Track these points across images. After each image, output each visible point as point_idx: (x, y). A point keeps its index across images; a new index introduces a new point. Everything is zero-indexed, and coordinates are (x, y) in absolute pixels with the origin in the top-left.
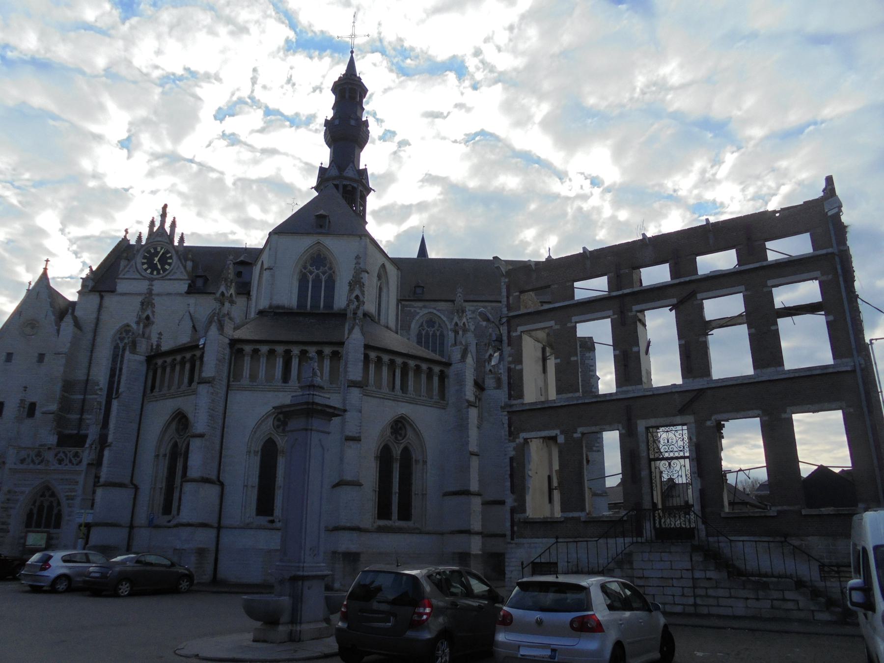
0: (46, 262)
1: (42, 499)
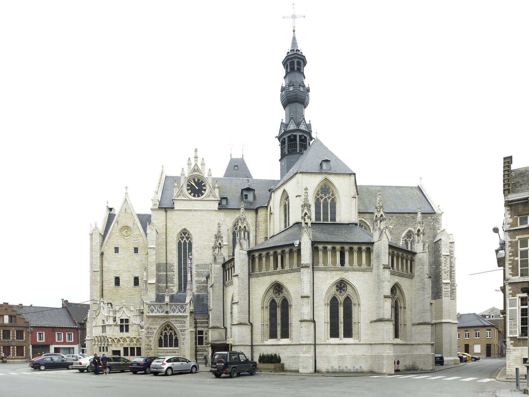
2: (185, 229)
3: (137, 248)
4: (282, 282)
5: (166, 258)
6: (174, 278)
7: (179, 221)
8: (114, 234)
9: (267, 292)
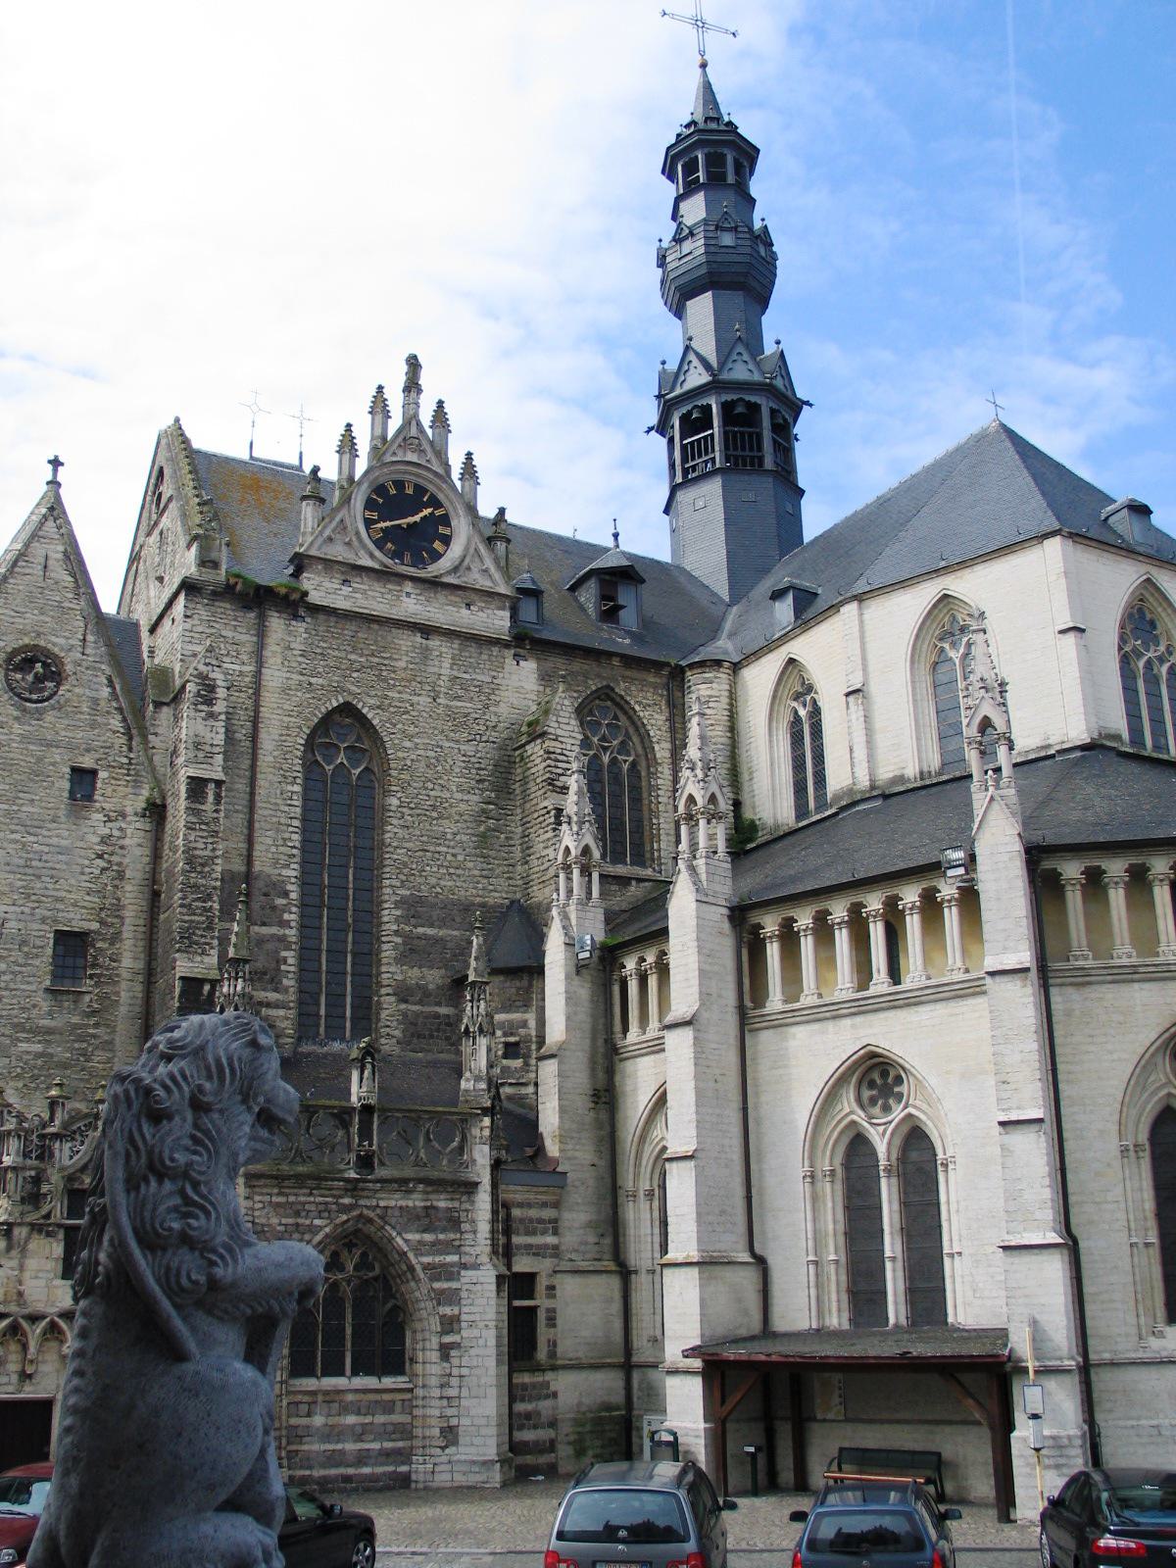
9: (1144, 1067)
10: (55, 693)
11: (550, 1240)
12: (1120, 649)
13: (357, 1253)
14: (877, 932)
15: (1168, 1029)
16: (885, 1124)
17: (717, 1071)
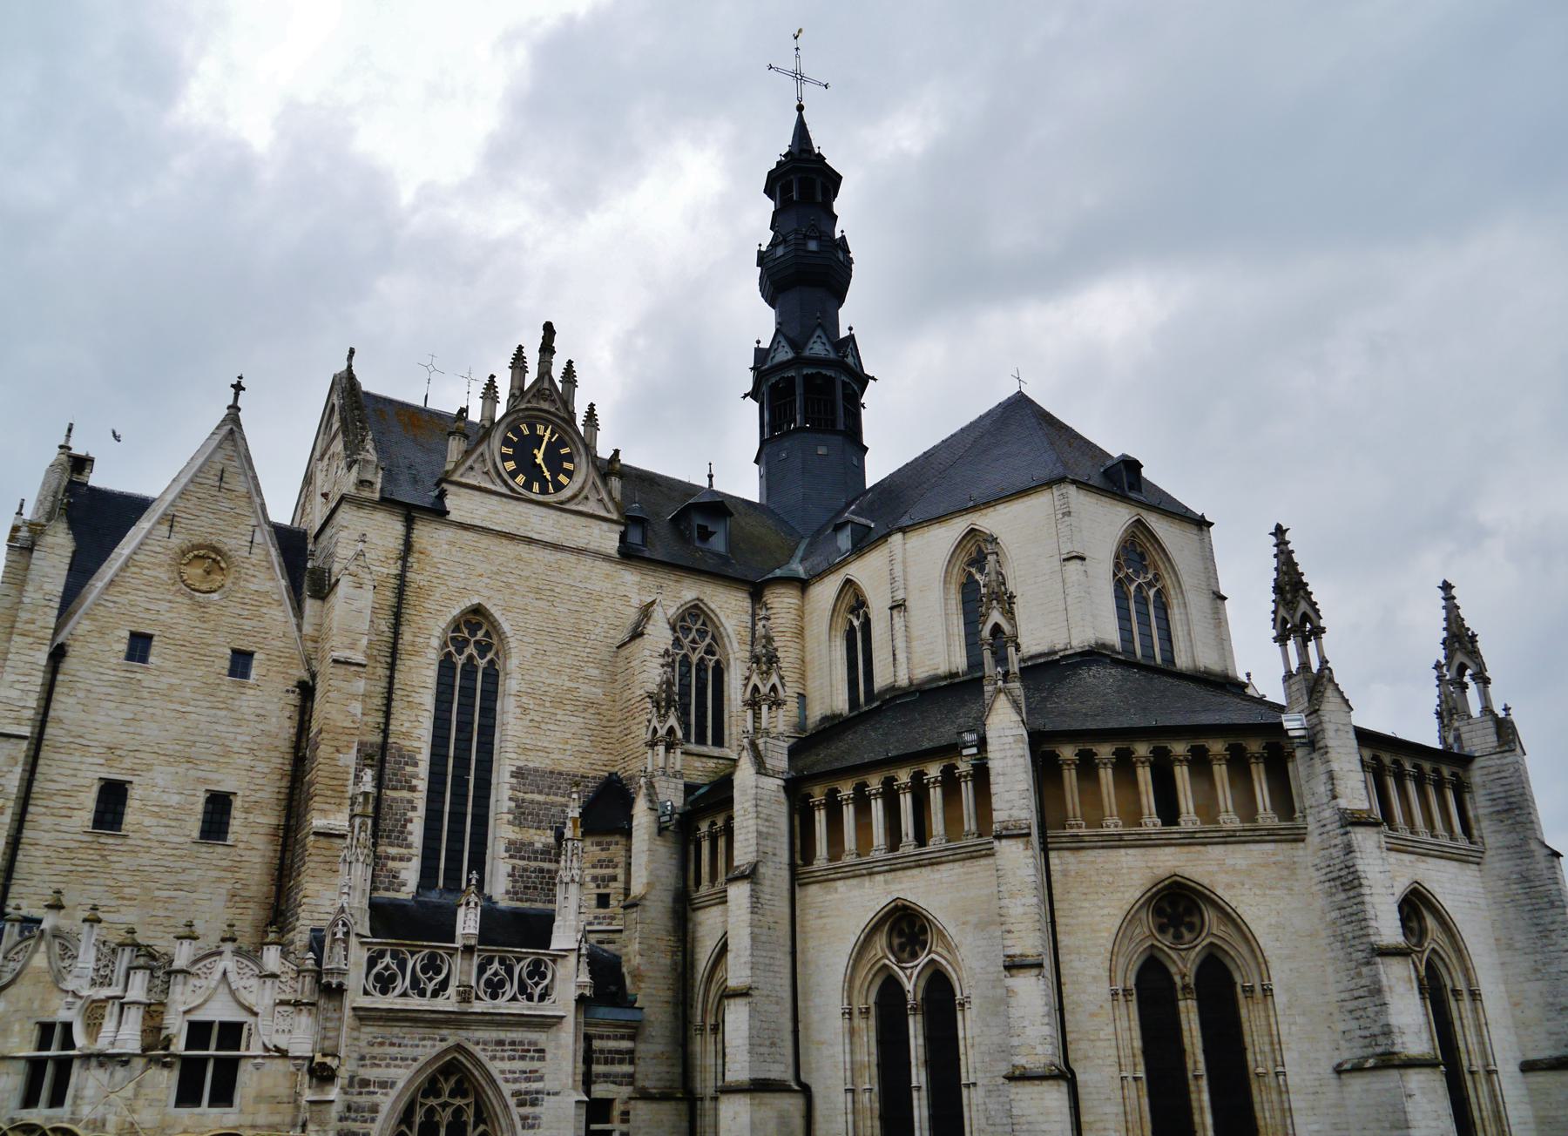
0: (233, 390)
1: (432, 1102)
2: (478, 610)
3: (249, 655)
4: (1206, 882)
5: (387, 724)
6: (411, 821)
7: (460, 570)
8: (142, 568)
9: (1130, 919)
10: (223, 585)
11: (626, 1068)
12: (1115, 575)
13: (453, 1081)
14: (906, 802)
15: (1150, 889)
16: (912, 967)
17: (771, 919)
